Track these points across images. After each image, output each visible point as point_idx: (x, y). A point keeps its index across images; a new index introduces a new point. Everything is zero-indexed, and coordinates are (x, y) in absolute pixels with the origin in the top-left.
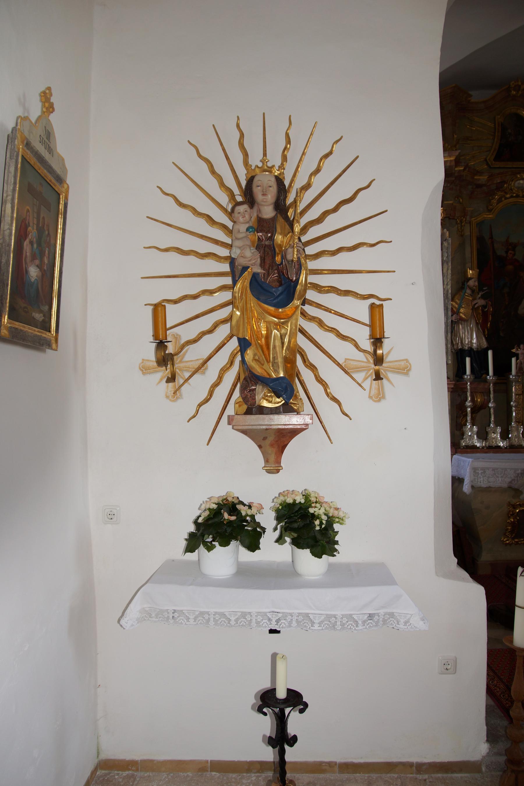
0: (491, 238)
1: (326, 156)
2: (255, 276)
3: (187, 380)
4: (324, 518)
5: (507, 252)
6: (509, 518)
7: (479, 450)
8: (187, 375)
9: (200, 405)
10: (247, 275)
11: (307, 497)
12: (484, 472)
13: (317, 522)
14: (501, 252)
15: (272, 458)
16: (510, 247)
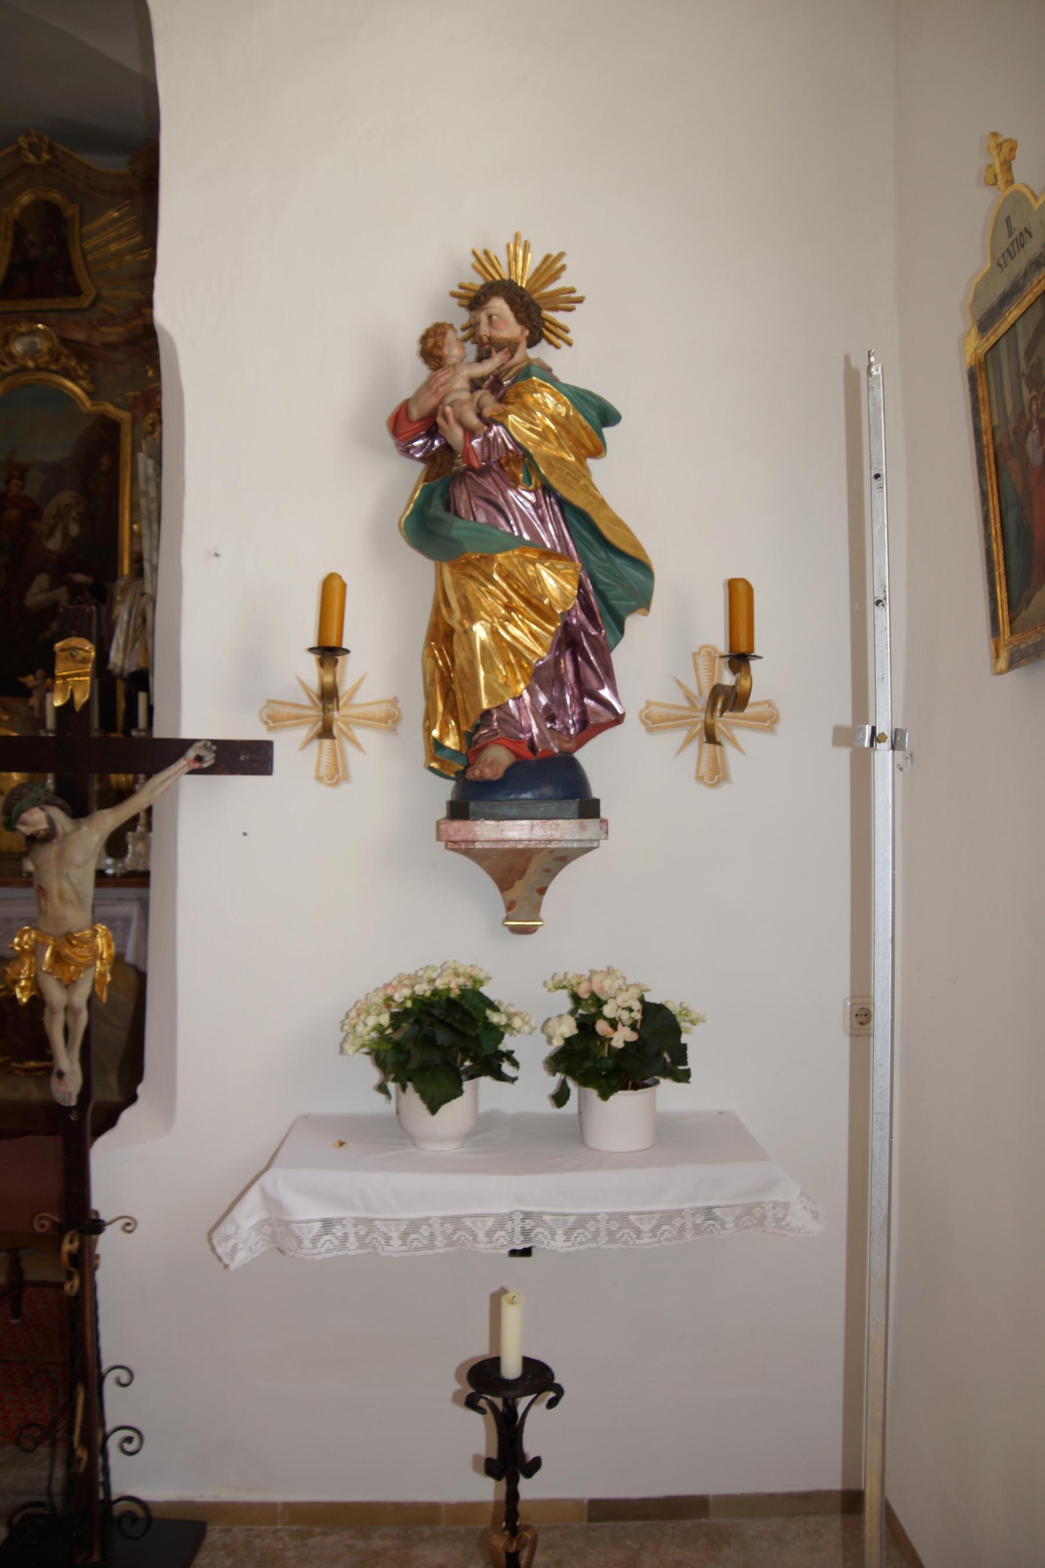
5: (8, 483)
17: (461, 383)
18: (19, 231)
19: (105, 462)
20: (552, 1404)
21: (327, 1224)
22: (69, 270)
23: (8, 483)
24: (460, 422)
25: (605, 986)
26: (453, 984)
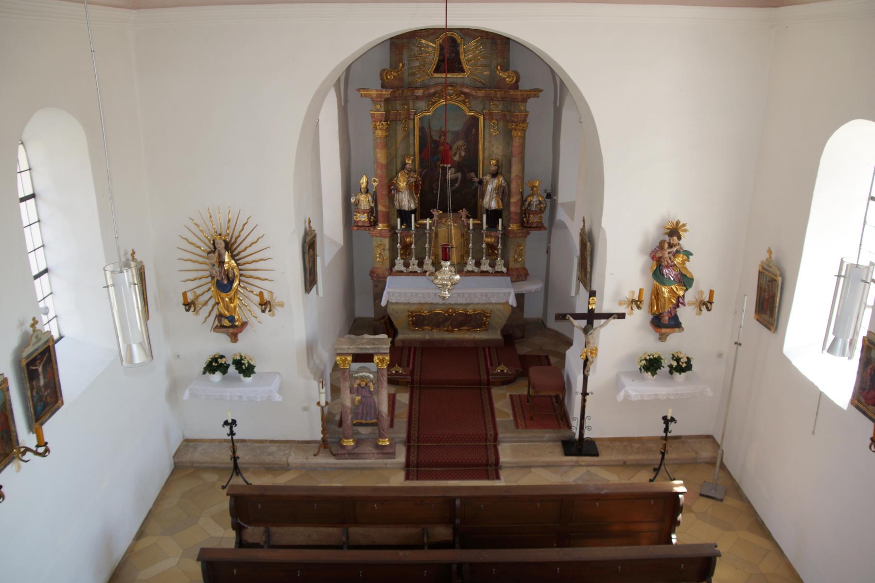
0: (430, 128)
1: (245, 224)
2: (217, 280)
3: (200, 309)
4: (247, 365)
5: (440, 137)
7: (403, 274)
8: (200, 306)
9: (206, 318)
10: (216, 279)
11: (241, 356)
13: (243, 367)
14: (436, 137)
15: (233, 339)
16: (442, 134)
17: (667, 253)
18: (442, 48)
19: (474, 131)
20: (675, 423)
21: (636, 395)
22: (460, 63)
23: (440, 137)
24: (667, 261)
25: (681, 356)
26: (656, 356)
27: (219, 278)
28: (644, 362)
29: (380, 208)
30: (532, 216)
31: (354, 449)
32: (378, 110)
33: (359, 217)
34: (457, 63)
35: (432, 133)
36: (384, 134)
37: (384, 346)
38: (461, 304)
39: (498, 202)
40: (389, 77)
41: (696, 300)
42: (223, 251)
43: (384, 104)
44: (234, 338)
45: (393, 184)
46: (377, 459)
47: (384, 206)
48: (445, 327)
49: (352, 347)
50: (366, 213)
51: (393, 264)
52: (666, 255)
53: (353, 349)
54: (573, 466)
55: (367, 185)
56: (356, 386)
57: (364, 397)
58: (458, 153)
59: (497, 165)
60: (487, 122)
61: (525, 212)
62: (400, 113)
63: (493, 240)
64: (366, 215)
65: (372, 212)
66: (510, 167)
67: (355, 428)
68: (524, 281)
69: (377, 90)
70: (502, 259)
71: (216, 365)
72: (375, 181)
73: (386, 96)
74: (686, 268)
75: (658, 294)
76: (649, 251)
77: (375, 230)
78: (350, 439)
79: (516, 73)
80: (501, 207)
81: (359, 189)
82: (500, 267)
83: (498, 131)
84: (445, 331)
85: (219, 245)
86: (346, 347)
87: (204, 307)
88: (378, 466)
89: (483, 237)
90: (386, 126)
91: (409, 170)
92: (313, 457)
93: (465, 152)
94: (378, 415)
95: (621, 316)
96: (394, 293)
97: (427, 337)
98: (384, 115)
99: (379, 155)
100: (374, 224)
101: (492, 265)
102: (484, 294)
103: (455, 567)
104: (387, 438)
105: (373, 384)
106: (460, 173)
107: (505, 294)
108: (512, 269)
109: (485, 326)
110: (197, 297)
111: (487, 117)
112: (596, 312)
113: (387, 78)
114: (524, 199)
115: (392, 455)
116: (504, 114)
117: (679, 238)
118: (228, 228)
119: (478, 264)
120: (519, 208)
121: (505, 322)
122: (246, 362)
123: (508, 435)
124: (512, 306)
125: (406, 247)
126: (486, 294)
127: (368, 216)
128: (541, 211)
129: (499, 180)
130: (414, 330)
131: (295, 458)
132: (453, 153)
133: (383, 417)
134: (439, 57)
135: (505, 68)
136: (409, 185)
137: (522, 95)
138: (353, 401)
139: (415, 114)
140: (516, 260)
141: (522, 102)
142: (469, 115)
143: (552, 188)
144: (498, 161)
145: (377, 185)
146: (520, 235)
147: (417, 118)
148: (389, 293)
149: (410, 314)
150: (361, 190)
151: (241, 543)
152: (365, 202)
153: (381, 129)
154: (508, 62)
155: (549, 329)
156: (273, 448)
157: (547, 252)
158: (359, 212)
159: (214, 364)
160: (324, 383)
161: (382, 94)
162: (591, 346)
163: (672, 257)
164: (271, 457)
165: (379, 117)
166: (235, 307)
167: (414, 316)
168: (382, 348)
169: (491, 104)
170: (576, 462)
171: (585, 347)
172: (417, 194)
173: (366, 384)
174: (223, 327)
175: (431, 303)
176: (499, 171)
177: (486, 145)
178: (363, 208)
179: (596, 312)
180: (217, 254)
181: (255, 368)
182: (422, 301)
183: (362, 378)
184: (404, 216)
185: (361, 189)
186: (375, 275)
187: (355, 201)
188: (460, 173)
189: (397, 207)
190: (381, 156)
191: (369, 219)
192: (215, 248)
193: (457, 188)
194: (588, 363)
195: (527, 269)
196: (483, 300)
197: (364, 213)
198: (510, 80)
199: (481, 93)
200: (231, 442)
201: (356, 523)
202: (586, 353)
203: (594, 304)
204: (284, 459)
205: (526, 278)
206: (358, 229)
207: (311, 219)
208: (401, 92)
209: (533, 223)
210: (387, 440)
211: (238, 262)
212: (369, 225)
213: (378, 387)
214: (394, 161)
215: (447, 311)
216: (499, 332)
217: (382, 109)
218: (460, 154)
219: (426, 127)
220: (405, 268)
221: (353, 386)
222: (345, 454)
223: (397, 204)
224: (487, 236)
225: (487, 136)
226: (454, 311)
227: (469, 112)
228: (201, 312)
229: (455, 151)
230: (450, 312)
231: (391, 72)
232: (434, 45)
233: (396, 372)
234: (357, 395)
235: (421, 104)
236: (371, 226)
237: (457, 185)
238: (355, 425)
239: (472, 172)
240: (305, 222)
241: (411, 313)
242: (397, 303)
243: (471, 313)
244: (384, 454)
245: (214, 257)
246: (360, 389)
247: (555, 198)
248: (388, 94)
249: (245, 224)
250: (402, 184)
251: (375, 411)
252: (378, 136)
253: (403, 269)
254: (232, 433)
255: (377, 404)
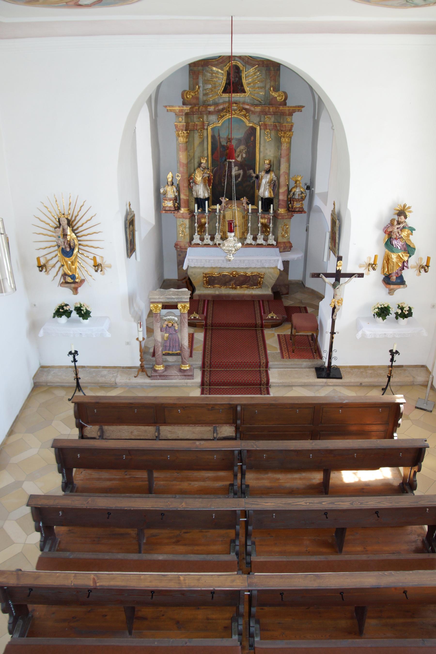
0: (219, 136)
1: (82, 206)
2: (62, 248)
3: (50, 270)
4: (85, 311)
5: (227, 143)
6: (204, 278)
7: (200, 246)
8: (50, 268)
9: (54, 277)
10: (61, 247)
12: (193, 261)
13: (82, 312)
14: (224, 143)
15: (75, 291)
18: (229, 74)
19: (252, 138)
21: (370, 334)
22: (242, 85)
24: (396, 234)
25: (404, 306)
26: (386, 306)
27: (64, 247)
28: (377, 310)
29: (182, 196)
30: (295, 203)
31: (163, 372)
32: (180, 122)
33: (167, 203)
34: (240, 85)
35: (221, 140)
36: (185, 140)
37: (186, 297)
38: (243, 268)
39: (270, 192)
40: (188, 96)
41: (417, 264)
42: (66, 226)
43: (185, 117)
44: (75, 291)
45: (192, 178)
46: (181, 379)
47: (185, 195)
48: (230, 285)
49: (161, 297)
50: (172, 200)
51: (192, 239)
52: (396, 230)
53: (162, 298)
54: (323, 386)
55: (172, 181)
56: (165, 326)
57: (171, 334)
58: (241, 154)
59: (270, 164)
60: (262, 131)
61: (290, 200)
62: (197, 124)
63: (266, 220)
64: (172, 201)
65: (176, 199)
66: (280, 166)
67: (165, 357)
68: (289, 251)
69: (179, 107)
70: (273, 234)
71: (63, 311)
72: (178, 176)
73: (186, 111)
74: (410, 240)
75: (388, 259)
76: (383, 227)
77: (179, 213)
78: (160, 365)
79: (285, 93)
80: (273, 196)
81: (167, 183)
82: (271, 241)
83: (270, 138)
84: (230, 288)
85: (63, 222)
86: (158, 297)
87: (53, 269)
88: (181, 385)
89: (259, 218)
90: (186, 134)
91: (204, 167)
92: (134, 378)
93: (246, 154)
94: (181, 348)
95: (361, 275)
96: (192, 260)
97: (217, 293)
98: (185, 126)
99: (181, 156)
100: (178, 209)
101: (266, 239)
102: (259, 261)
103: (236, 453)
104: (188, 364)
105: (178, 325)
106: (242, 170)
107: (275, 260)
108: (280, 243)
109: (260, 285)
110: (48, 261)
111: (263, 128)
112: (342, 272)
113: (187, 97)
114: (290, 190)
115: (191, 376)
116: (276, 125)
117: (406, 217)
118: (70, 209)
119: (255, 239)
120: (286, 197)
121: (275, 282)
122: (85, 308)
123: (276, 363)
124: (280, 270)
125: (202, 226)
126: (261, 261)
127: (173, 203)
128: (303, 199)
129: (271, 176)
130: (207, 288)
131: (121, 379)
132: (237, 155)
133: (185, 349)
134: (226, 81)
135: (277, 89)
136: (204, 179)
137: (289, 110)
138: (163, 337)
139: (208, 125)
140: (283, 236)
141: (288, 115)
142: (248, 126)
143: (311, 182)
144: (270, 161)
145: (180, 179)
146: (286, 217)
147: (210, 128)
148: (189, 260)
149: (204, 275)
150: (168, 183)
151: (82, 436)
152: (171, 192)
153: (182, 136)
154: (279, 85)
155: (307, 288)
156: (105, 372)
157: (306, 230)
158: (166, 200)
159: (61, 310)
160: (141, 324)
161: (183, 109)
162: (338, 297)
163: (400, 232)
164: (103, 378)
165: (181, 128)
166: (76, 268)
167: (208, 277)
168: (184, 298)
169: (266, 117)
170: (326, 383)
171: (334, 298)
172: (209, 186)
173: (172, 325)
174: (67, 283)
175: (220, 268)
176: (271, 169)
177: (262, 149)
178: (169, 197)
179: (342, 272)
180: (61, 229)
181: (91, 313)
182: (214, 266)
183: (169, 320)
184: (200, 202)
185: (167, 182)
186: (179, 247)
187: (164, 191)
188: (242, 170)
189: (195, 196)
190: (183, 157)
191: (174, 205)
192: (60, 224)
193: (239, 181)
194: (336, 310)
195: (291, 242)
196: (259, 265)
197: (170, 200)
198: (280, 98)
199: (258, 109)
200: (74, 367)
201: (165, 423)
202: (334, 302)
203: (340, 266)
204: (113, 380)
205: (291, 250)
206: (166, 213)
207: (131, 203)
208: (197, 108)
209: (296, 208)
210: (188, 365)
211: (77, 235)
212: (174, 209)
213: (181, 327)
214: (192, 161)
215: (232, 274)
216: (270, 289)
217: (184, 121)
218: (242, 155)
219: (217, 135)
220: (201, 242)
221: (162, 326)
222: (157, 376)
223: (194, 193)
224: (262, 218)
225: (262, 142)
226: (237, 274)
227: (249, 124)
228: (50, 272)
229: (238, 154)
230: (234, 274)
231: (190, 92)
232: (222, 72)
233: (194, 317)
234: (166, 333)
235: (213, 118)
236: (176, 210)
237: (240, 179)
238: (164, 355)
239: (251, 169)
240: (127, 205)
241: (206, 274)
242: (195, 267)
243: (250, 275)
244: (185, 375)
245: (60, 231)
246: (168, 328)
247: (313, 189)
248: (188, 110)
249: (82, 206)
250: (199, 179)
251: (179, 345)
252: (180, 142)
253: (199, 242)
254: (75, 361)
255: (180, 339)
